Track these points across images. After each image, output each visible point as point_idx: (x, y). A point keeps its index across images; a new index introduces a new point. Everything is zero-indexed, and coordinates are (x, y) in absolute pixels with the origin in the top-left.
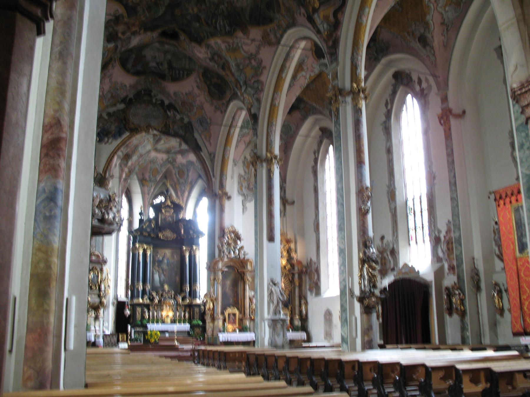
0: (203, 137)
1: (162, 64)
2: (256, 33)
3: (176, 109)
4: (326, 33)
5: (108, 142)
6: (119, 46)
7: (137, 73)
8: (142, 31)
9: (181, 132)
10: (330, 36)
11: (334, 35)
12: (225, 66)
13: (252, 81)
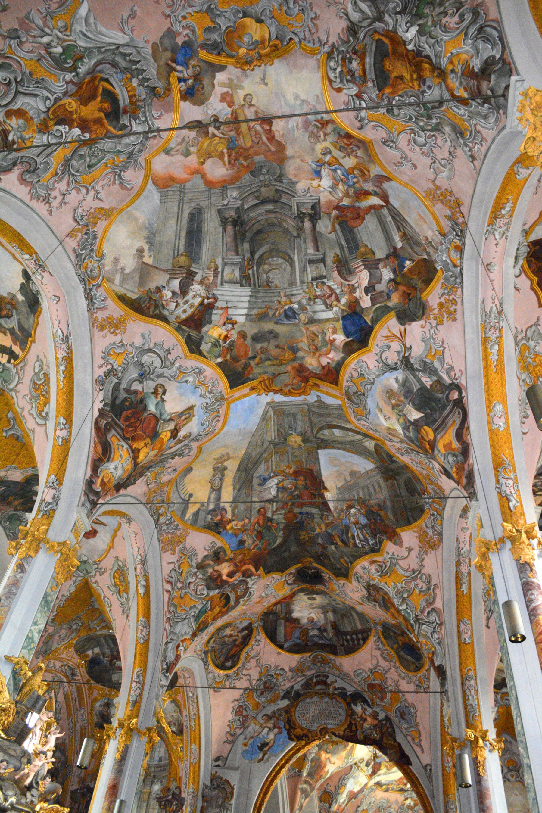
0: (409, 738)
1: (325, 630)
2: (409, 536)
3: (365, 701)
4: (454, 469)
5: (262, 759)
6: (232, 597)
7: (295, 649)
8: (261, 571)
9: (376, 736)
10: (460, 469)
11: (466, 467)
12: (386, 603)
13: (426, 614)
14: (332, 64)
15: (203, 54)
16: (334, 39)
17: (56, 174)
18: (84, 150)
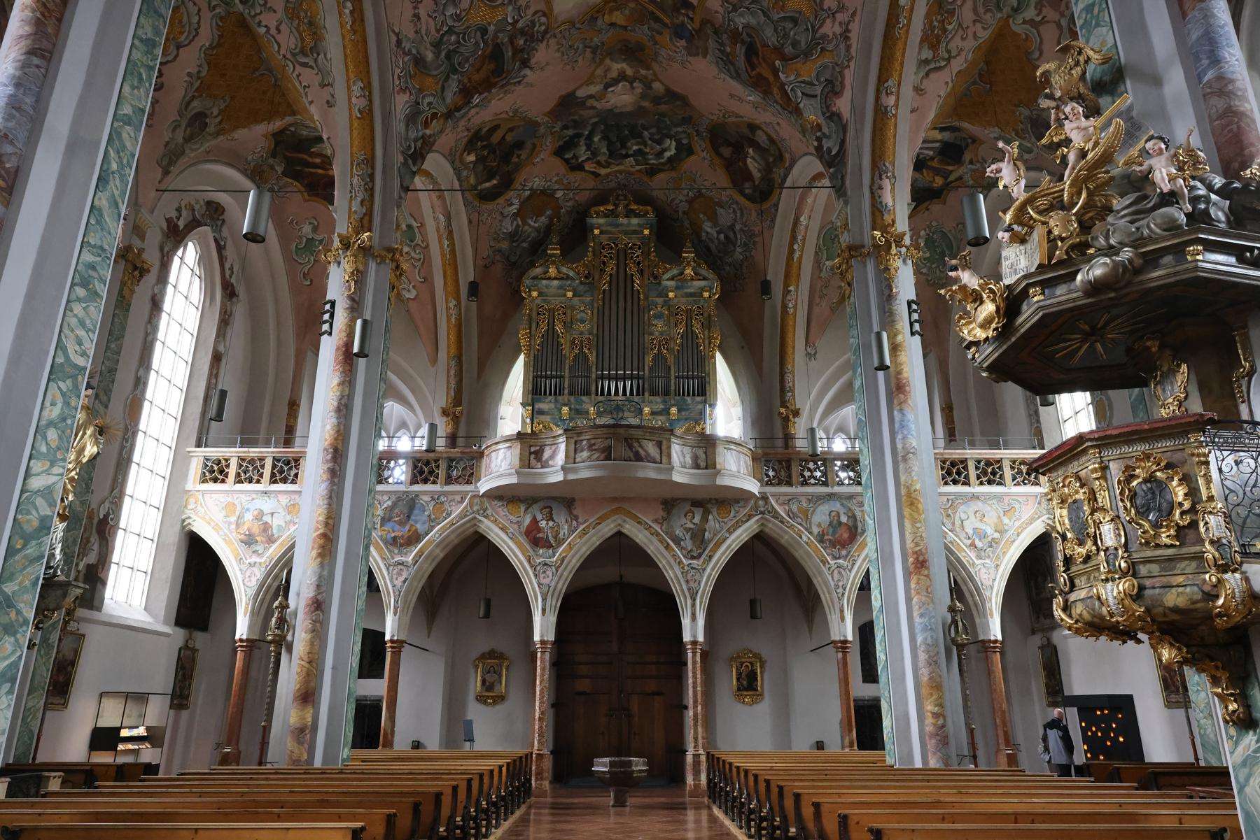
14: (543, 28)
15: (666, 20)
16: (542, 46)
17: (822, 49)
18: (788, 50)
